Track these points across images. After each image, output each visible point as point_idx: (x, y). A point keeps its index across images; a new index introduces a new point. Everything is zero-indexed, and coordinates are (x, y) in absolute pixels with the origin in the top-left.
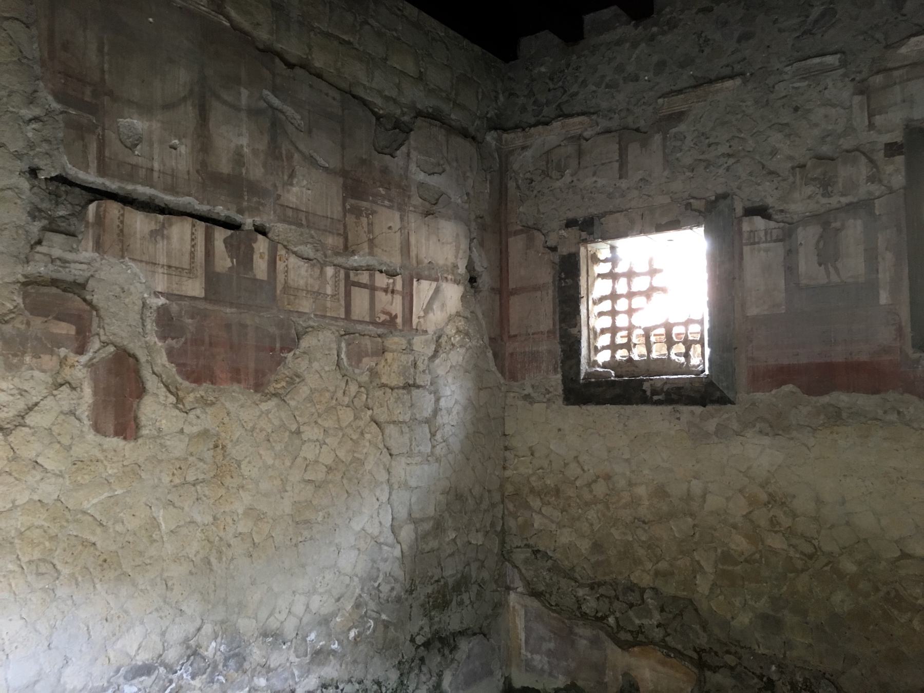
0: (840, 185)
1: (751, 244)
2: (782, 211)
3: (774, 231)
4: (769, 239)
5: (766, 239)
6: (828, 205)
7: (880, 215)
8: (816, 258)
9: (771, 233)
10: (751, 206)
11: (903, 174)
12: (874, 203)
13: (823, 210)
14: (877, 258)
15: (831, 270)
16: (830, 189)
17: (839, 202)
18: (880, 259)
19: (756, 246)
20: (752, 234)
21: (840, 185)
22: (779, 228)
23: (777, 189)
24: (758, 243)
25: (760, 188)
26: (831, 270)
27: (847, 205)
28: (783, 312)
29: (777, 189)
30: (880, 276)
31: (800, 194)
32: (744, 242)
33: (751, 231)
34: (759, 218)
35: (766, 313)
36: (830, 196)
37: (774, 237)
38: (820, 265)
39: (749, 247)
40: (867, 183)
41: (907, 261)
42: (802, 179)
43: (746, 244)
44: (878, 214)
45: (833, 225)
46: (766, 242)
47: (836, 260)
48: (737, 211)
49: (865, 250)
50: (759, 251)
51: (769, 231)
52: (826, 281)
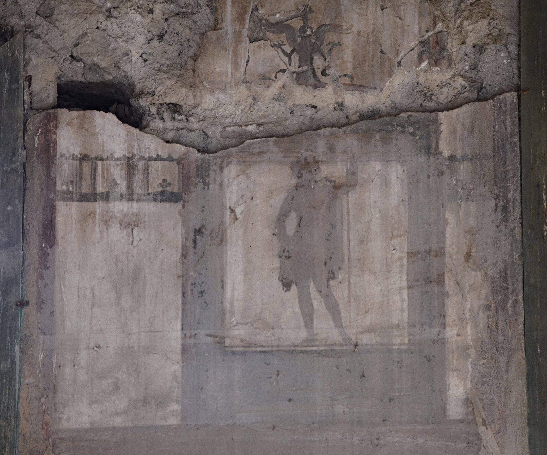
0: (348, 54)
1: (84, 198)
2: (175, 108)
3: (152, 163)
4: (138, 190)
5: (129, 187)
6: (310, 112)
7: (452, 158)
8: (276, 263)
9: (146, 170)
10: (79, 78)
11: (513, 48)
12: (436, 122)
13: (293, 123)
14: (440, 281)
15: (318, 303)
16: (318, 62)
17: (340, 106)
18: (449, 284)
19: (99, 207)
20: (87, 168)
21: (348, 54)
22: (170, 159)
23: (161, 37)
24: (106, 197)
25: (112, 26)
26: (318, 303)
27: (363, 117)
28: (173, 421)
29: (161, 37)
30: (451, 333)
31: (236, 64)
32: (61, 187)
33: (84, 158)
34: (111, 117)
35: (118, 422)
36: (318, 85)
37: (155, 188)
38: (287, 285)
39: (75, 204)
40: (420, 61)
41: (520, 297)
42: (240, 19)
43: (68, 197)
44: (446, 154)
45: (325, 170)
46: (130, 196)
47: (332, 276)
48: (36, 86)
49: (412, 255)
50: (107, 223)
51: (141, 164)
52: (303, 334)
